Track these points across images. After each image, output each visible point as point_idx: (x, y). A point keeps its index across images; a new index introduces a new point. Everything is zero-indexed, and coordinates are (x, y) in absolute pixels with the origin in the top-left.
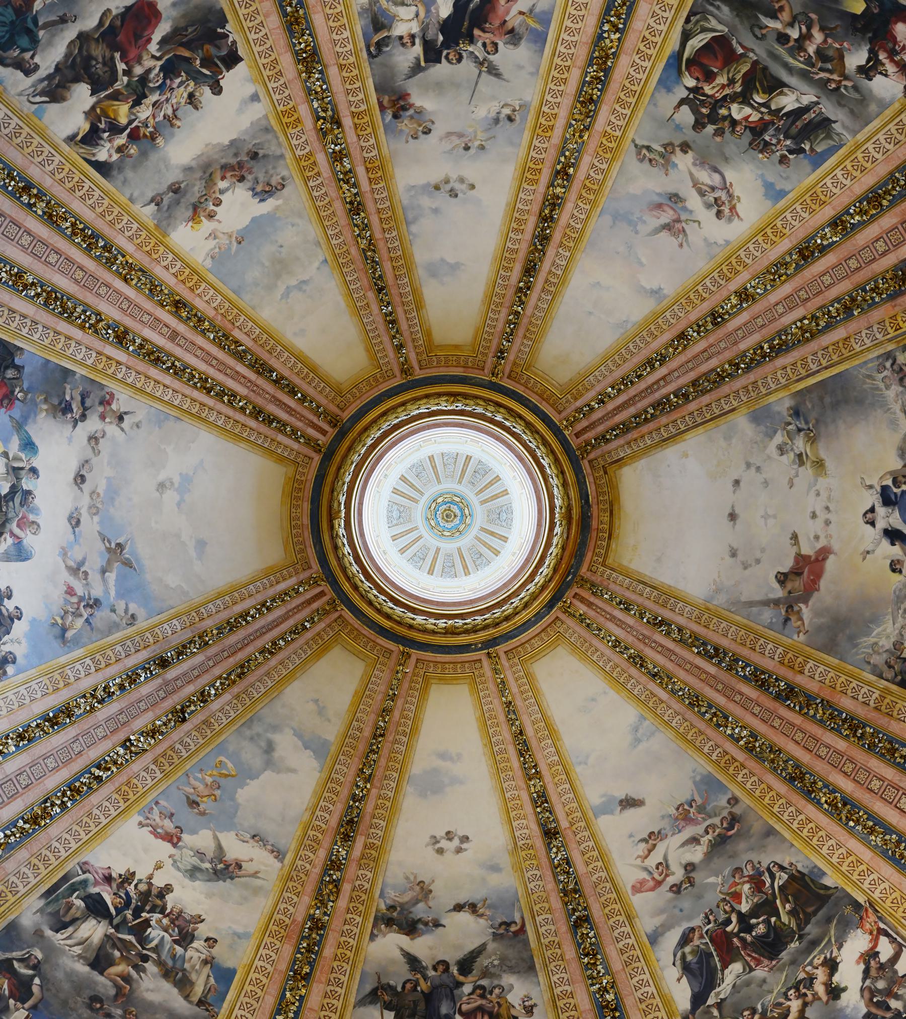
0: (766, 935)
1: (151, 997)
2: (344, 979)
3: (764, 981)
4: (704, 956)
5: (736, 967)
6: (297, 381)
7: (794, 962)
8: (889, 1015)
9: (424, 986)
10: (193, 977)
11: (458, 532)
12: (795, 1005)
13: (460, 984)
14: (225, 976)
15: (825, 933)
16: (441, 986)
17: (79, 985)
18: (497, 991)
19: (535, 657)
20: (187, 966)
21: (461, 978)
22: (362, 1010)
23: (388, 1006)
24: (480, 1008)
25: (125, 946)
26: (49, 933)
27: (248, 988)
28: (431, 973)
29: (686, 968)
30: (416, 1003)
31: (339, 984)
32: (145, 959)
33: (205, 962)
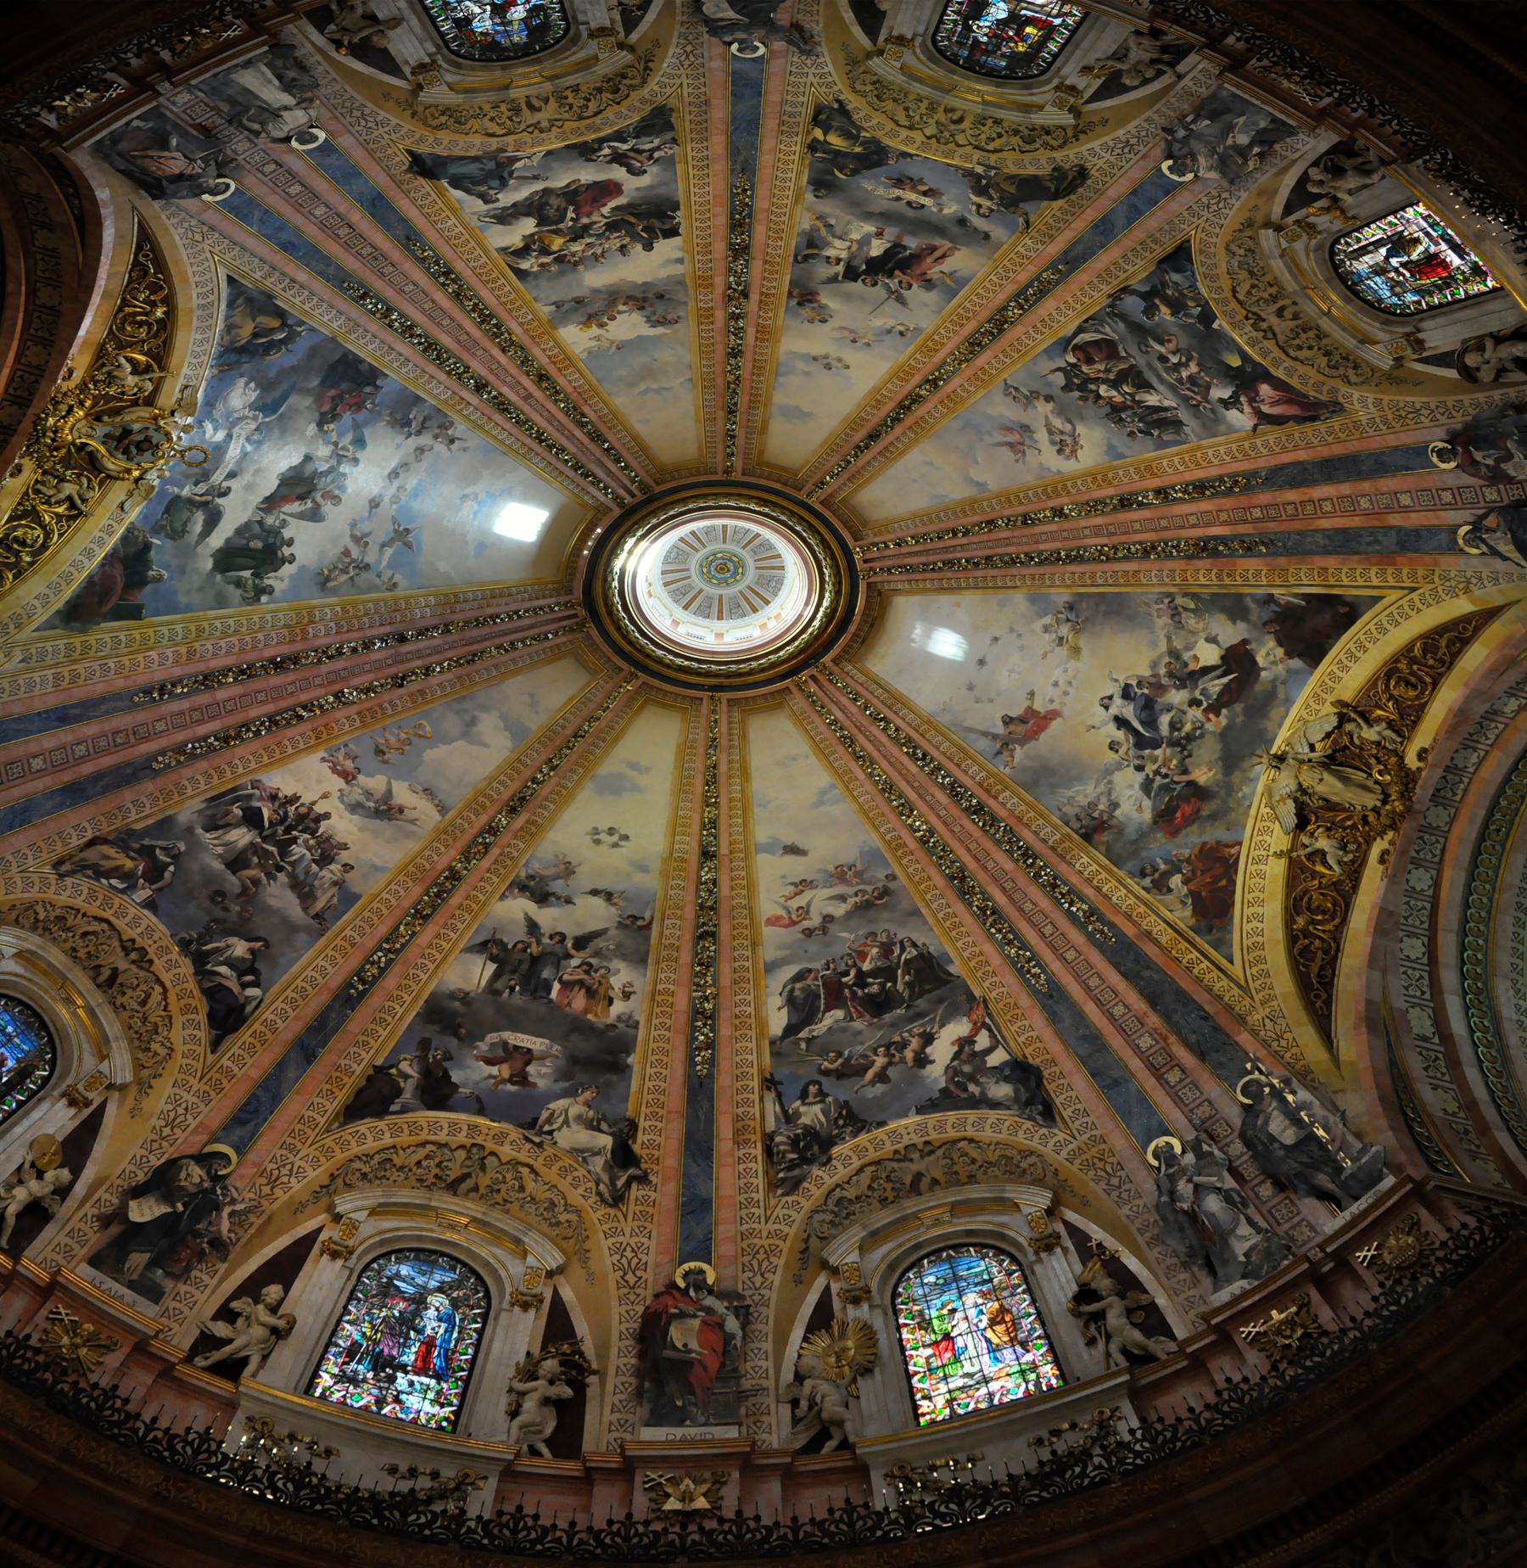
6: (625, 453)
8: (964, 1095)
11: (724, 583)
19: (753, 711)
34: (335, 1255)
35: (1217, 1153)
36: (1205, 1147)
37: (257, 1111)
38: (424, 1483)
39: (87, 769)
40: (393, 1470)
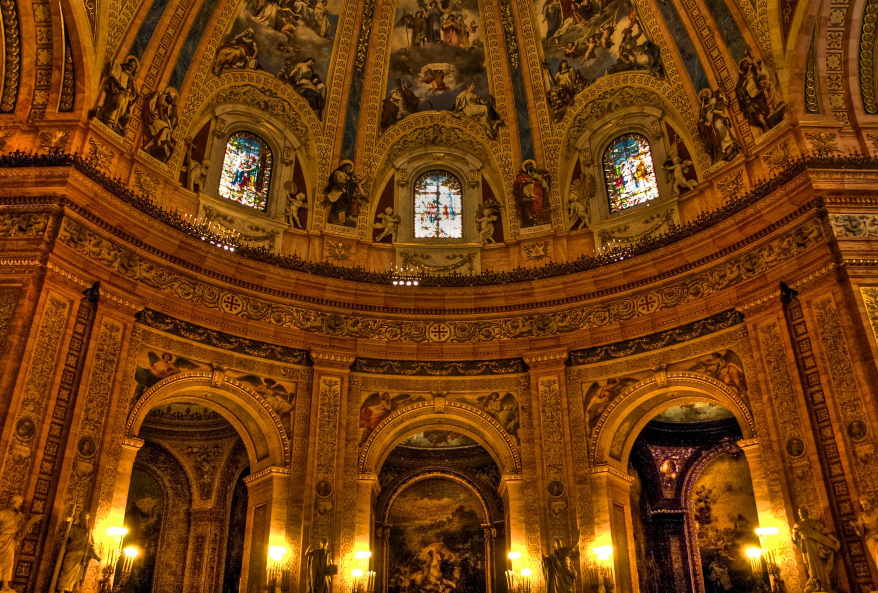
0: (586, 7)
1: (304, 37)
2: (388, 15)
3: (581, 30)
4: (557, 11)
5: (570, 20)
7: (596, 24)
9: (426, 15)
10: (320, 23)
12: (591, 45)
13: (442, 14)
14: (333, 19)
15: (613, 13)
16: (434, 14)
17: (273, 40)
18: (460, 18)
20: (316, 18)
21: (443, 10)
22: (398, 29)
23: (409, 26)
24: (452, 27)
25: (287, 14)
26: (253, 18)
27: (345, 26)
28: (429, 8)
29: (548, 16)
30: (422, 24)
31: (387, 18)
32: (297, 18)
33: (324, 14)
34: (403, 186)
35: (725, 99)
36: (721, 96)
37: (349, 141)
38: (459, 259)
39: (190, 21)
40: (448, 257)
